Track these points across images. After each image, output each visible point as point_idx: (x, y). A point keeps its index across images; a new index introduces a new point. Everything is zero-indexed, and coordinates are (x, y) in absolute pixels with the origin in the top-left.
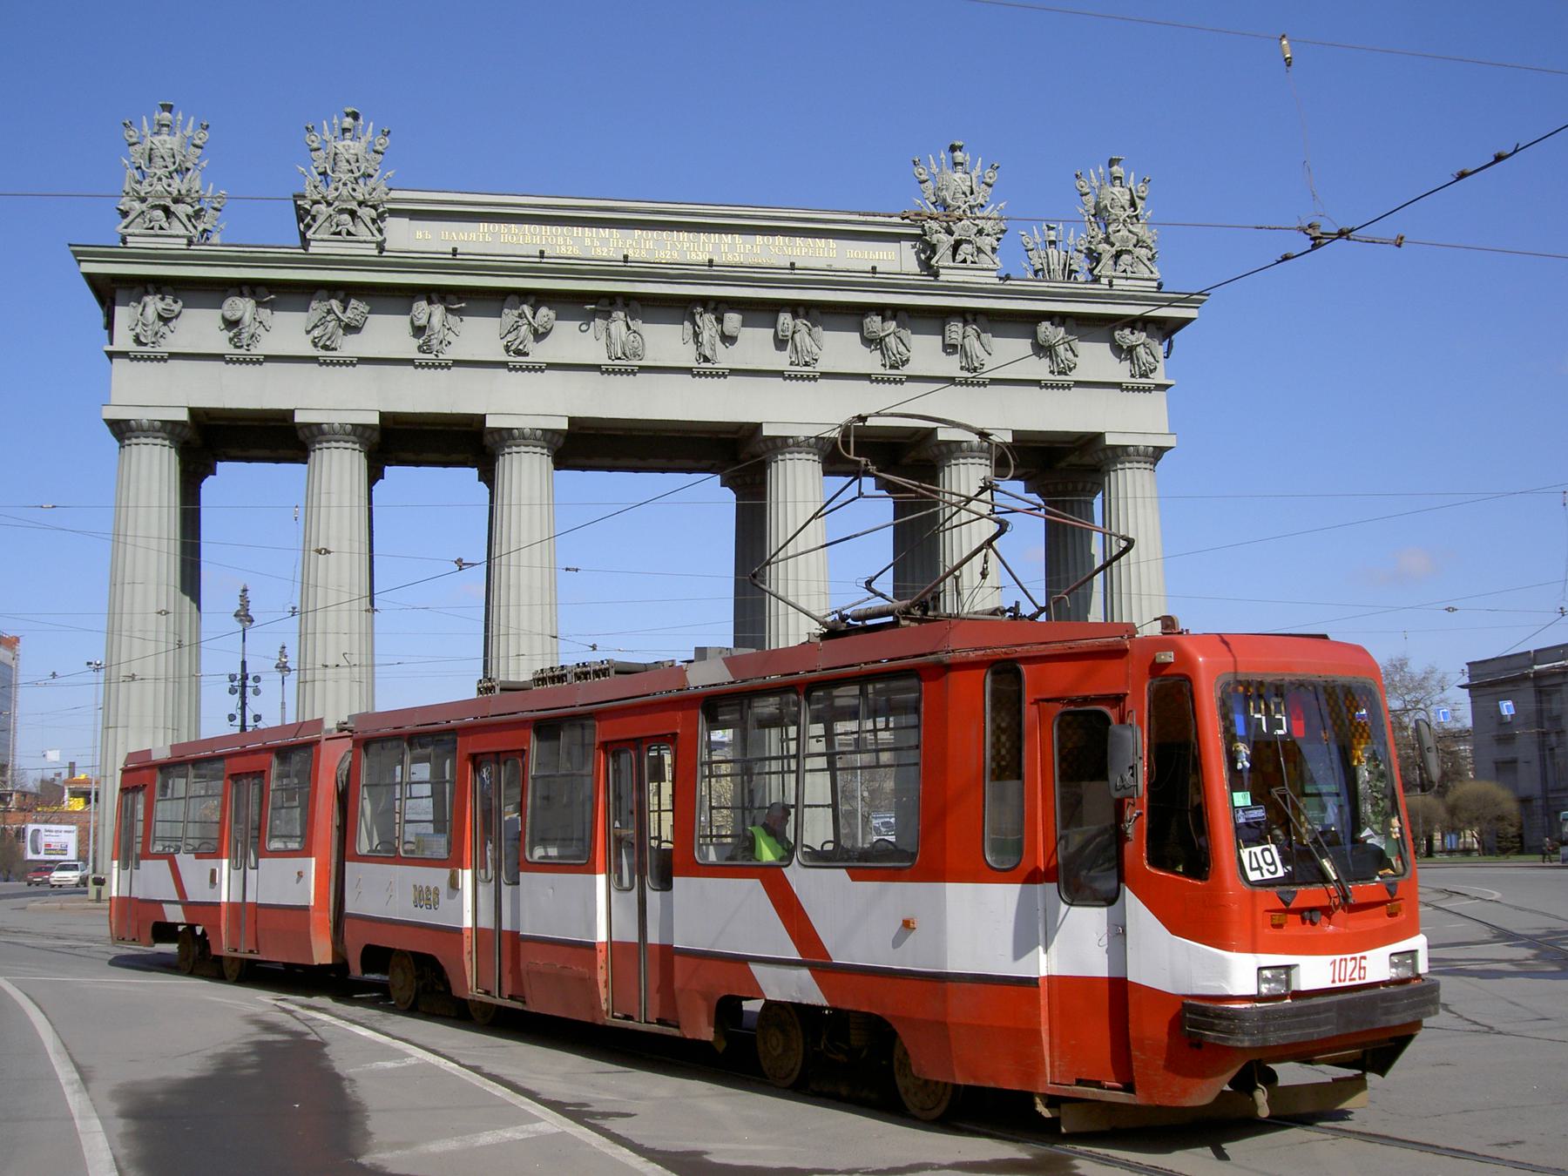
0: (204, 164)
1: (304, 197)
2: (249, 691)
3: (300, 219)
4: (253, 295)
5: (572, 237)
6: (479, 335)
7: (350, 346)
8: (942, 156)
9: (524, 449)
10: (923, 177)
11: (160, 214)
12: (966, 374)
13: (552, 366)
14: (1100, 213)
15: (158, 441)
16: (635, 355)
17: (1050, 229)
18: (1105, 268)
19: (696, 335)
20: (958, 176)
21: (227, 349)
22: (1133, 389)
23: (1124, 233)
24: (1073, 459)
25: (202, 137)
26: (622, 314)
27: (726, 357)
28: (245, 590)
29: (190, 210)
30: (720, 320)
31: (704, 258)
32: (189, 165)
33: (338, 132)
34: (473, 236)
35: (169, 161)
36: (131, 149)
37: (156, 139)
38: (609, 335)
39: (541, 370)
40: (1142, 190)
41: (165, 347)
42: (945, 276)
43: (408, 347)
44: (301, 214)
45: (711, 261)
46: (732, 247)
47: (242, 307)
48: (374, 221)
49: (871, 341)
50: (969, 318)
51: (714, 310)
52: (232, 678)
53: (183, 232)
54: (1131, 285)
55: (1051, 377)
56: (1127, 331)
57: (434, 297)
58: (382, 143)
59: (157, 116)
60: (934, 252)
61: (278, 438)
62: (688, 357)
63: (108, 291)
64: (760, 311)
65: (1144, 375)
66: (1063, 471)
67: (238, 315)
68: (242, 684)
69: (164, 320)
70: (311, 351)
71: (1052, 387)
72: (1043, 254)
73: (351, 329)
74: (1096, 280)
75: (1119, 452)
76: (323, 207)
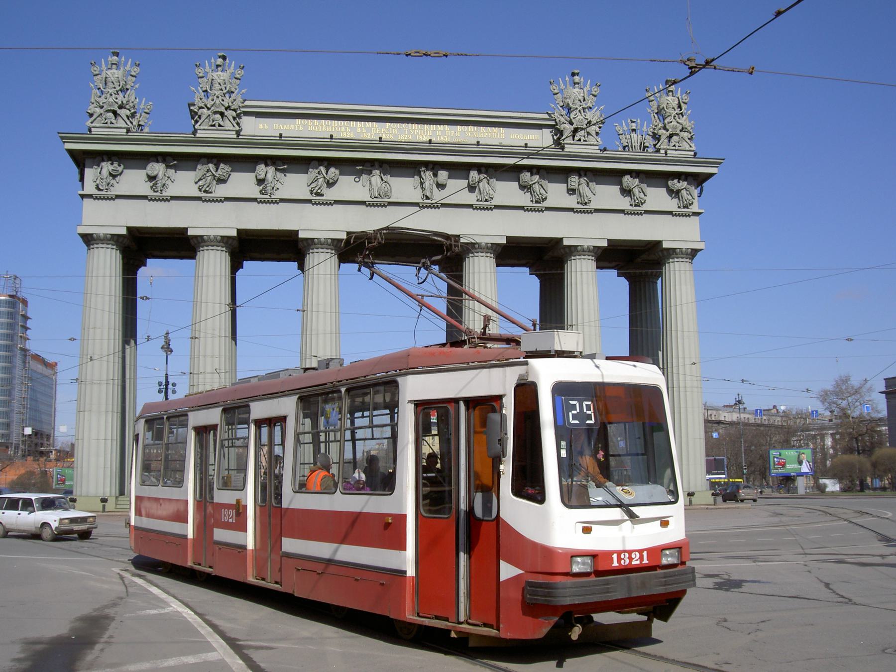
0: (137, 86)
1: (194, 105)
2: (170, 391)
3: (193, 118)
4: (164, 161)
5: (350, 127)
6: (295, 184)
7: (220, 191)
8: (567, 79)
9: (321, 250)
10: (556, 91)
11: (111, 115)
12: (580, 206)
13: (337, 202)
14: (660, 112)
15: (110, 246)
16: (386, 195)
17: (632, 122)
18: (663, 144)
19: (422, 184)
20: (576, 90)
21: (149, 192)
22: (679, 215)
23: (674, 123)
24: (644, 256)
25: (135, 71)
26: (378, 172)
27: (438, 196)
28: (167, 334)
29: (128, 113)
30: (435, 175)
31: (426, 139)
32: (128, 87)
33: (213, 67)
34: (292, 127)
35: (116, 84)
36: (95, 78)
37: (109, 72)
38: (371, 184)
39: (331, 204)
40: (685, 98)
41: (114, 191)
42: (568, 149)
43: (254, 191)
44: (193, 114)
45: (430, 141)
46: (444, 132)
47: (157, 168)
48: (234, 118)
49: (525, 187)
50: (582, 173)
51: (432, 169)
52: (160, 384)
53: (124, 125)
54: (679, 154)
55: (631, 208)
56: (676, 181)
57: (269, 162)
58: (239, 73)
59: (110, 59)
60: (562, 135)
61: (179, 244)
62: (417, 197)
63: (82, 159)
64: (459, 170)
65: (686, 207)
66: (638, 264)
67: (155, 173)
68: (166, 387)
69: (114, 176)
70: (198, 194)
71: (631, 214)
72: (628, 137)
73: (221, 181)
74: (658, 151)
75: (671, 252)
76: (205, 110)
